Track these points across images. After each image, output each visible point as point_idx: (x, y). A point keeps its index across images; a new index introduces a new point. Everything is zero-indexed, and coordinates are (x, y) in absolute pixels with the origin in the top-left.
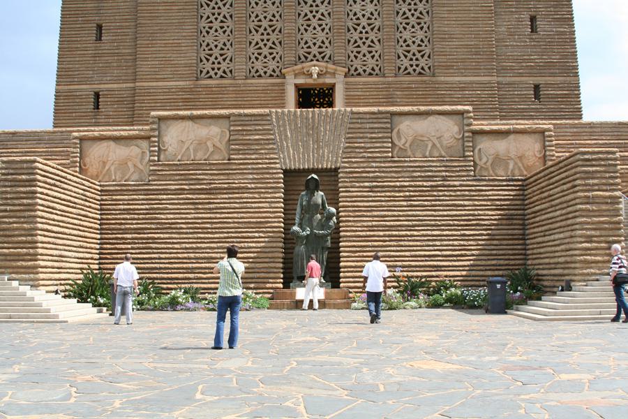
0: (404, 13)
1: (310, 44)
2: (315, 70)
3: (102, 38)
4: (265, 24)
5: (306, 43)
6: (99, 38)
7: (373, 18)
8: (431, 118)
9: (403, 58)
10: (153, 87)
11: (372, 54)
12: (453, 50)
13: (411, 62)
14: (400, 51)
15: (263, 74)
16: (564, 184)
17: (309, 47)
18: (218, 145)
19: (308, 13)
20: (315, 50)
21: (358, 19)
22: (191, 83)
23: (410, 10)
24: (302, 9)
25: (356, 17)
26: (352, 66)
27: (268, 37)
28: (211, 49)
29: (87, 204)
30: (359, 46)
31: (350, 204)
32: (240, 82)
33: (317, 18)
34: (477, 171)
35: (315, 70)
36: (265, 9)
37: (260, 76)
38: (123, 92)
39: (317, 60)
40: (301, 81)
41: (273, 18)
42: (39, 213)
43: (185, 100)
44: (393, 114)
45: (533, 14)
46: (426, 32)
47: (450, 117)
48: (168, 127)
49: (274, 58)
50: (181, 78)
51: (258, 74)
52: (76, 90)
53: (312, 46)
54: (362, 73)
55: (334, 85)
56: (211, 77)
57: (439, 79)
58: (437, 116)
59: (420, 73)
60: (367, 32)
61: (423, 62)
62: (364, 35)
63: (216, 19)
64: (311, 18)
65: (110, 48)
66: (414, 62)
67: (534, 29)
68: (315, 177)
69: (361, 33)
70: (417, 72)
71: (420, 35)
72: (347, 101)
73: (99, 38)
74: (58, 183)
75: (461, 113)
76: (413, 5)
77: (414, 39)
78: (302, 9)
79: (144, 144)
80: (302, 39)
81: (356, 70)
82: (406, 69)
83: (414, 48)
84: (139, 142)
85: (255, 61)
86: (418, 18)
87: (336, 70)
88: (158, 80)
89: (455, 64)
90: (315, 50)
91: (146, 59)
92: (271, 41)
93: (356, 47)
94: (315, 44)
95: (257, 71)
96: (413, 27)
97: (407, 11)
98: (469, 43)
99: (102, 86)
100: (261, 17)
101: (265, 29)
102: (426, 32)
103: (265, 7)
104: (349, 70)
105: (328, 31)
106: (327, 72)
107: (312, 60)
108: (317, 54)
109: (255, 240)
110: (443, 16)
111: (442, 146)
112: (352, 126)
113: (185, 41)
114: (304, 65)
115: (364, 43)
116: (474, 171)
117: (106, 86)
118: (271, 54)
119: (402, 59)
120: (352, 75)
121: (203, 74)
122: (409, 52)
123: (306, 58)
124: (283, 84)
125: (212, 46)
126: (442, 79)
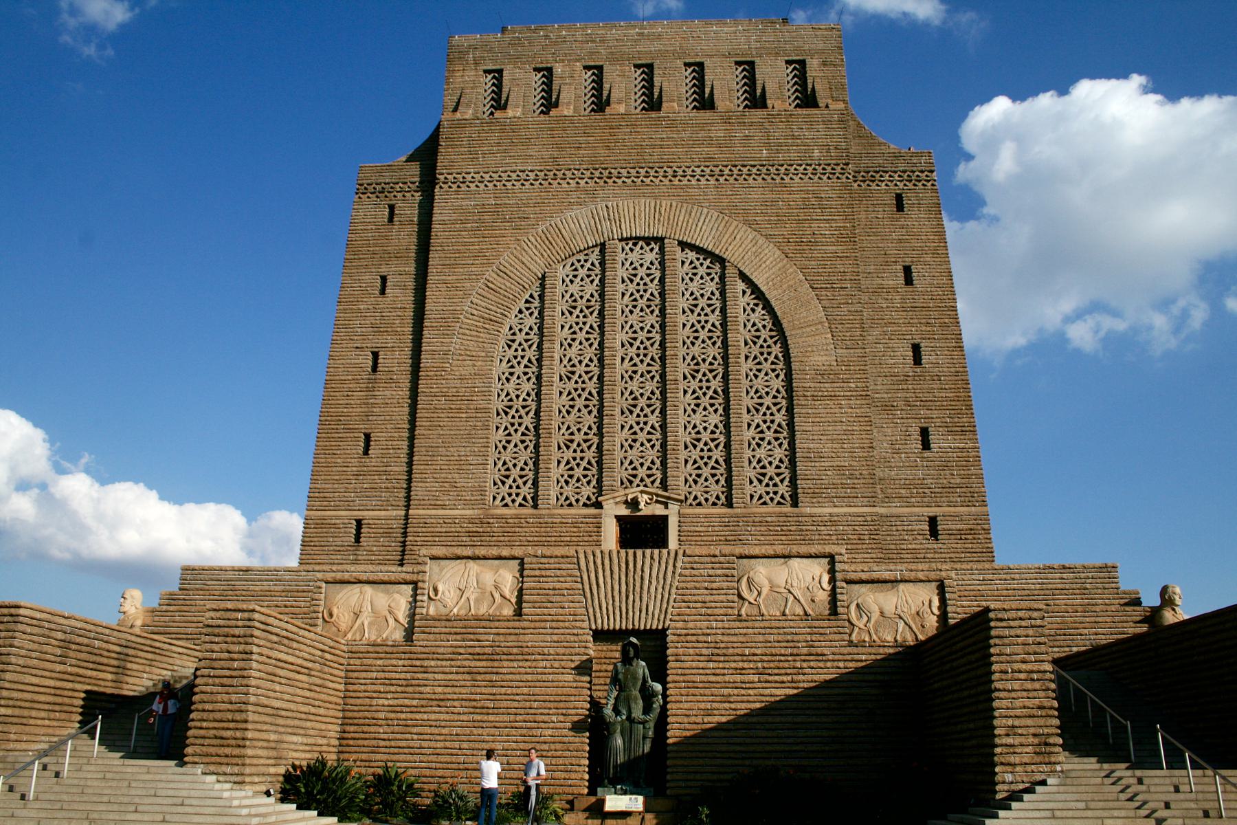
0: (758, 426)
3: (370, 452)
4: (578, 438)
5: (631, 463)
6: (366, 452)
8: (795, 563)
9: (756, 482)
10: (430, 516)
11: (716, 478)
12: (821, 472)
13: (768, 489)
14: (752, 474)
15: (574, 503)
16: (970, 653)
17: (635, 469)
18: (507, 594)
21: (698, 433)
22: (480, 512)
23: (765, 422)
24: (626, 419)
25: (696, 430)
26: (690, 493)
27: (582, 455)
28: (508, 469)
29: (326, 669)
30: (699, 468)
31: (681, 678)
32: (544, 512)
34: (854, 635)
35: (643, 499)
36: (579, 420)
37: (570, 505)
38: (393, 522)
39: (645, 486)
40: (624, 511)
41: (589, 431)
42: (253, 682)
43: (471, 534)
44: (740, 557)
45: (924, 425)
47: (818, 560)
48: (441, 570)
49: (589, 483)
50: (468, 504)
51: (568, 502)
52: (331, 517)
54: (703, 502)
55: (667, 516)
56: (506, 505)
57: (803, 510)
58: (799, 559)
59: (779, 503)
62: (706, 454)
63: (516, 431)
65: (376, 464)
66: (770, 489)
67: (926, 445)
68: (634, 640)
70: (776, 502)
73: (366, 452)
74: (286, 641)
75: (831, 558)
78: (626, 419)
79: (408, 589)
80: (625, 458)
81: (695, 498)
82: (761, 497)
83: (771, 471)
84: (404, 587)
85: (564, 484)
87: (669, 498)
88: (436, 507)
89: (825, 491)
91: (423, 480)
92: (586, 461)
94: (642, 465)
95: (567, 498)
96: (769, 443)
98: (843, 464)
99: (365, 513)
100: (574, 429)
101: (579, 445)
103: (579, 417)
104: (686, 498)
106: (657, 502)
107: (638, 486)
109: (551, 725)
110: (807, 429)
111: (806, 600)
112: (684, 571)
113: (475, 458)
114: (627, 491)
115: (706, 464)
116: (850, 635)
117: (371, 513)
118: (585, 476)
119: (754, 484)
120: (691, 505)
121: (498, 502)
122: (764, 475)
123: (631, 482)
124: (599, 516)
125: (510, 465)
126: (808, 510)
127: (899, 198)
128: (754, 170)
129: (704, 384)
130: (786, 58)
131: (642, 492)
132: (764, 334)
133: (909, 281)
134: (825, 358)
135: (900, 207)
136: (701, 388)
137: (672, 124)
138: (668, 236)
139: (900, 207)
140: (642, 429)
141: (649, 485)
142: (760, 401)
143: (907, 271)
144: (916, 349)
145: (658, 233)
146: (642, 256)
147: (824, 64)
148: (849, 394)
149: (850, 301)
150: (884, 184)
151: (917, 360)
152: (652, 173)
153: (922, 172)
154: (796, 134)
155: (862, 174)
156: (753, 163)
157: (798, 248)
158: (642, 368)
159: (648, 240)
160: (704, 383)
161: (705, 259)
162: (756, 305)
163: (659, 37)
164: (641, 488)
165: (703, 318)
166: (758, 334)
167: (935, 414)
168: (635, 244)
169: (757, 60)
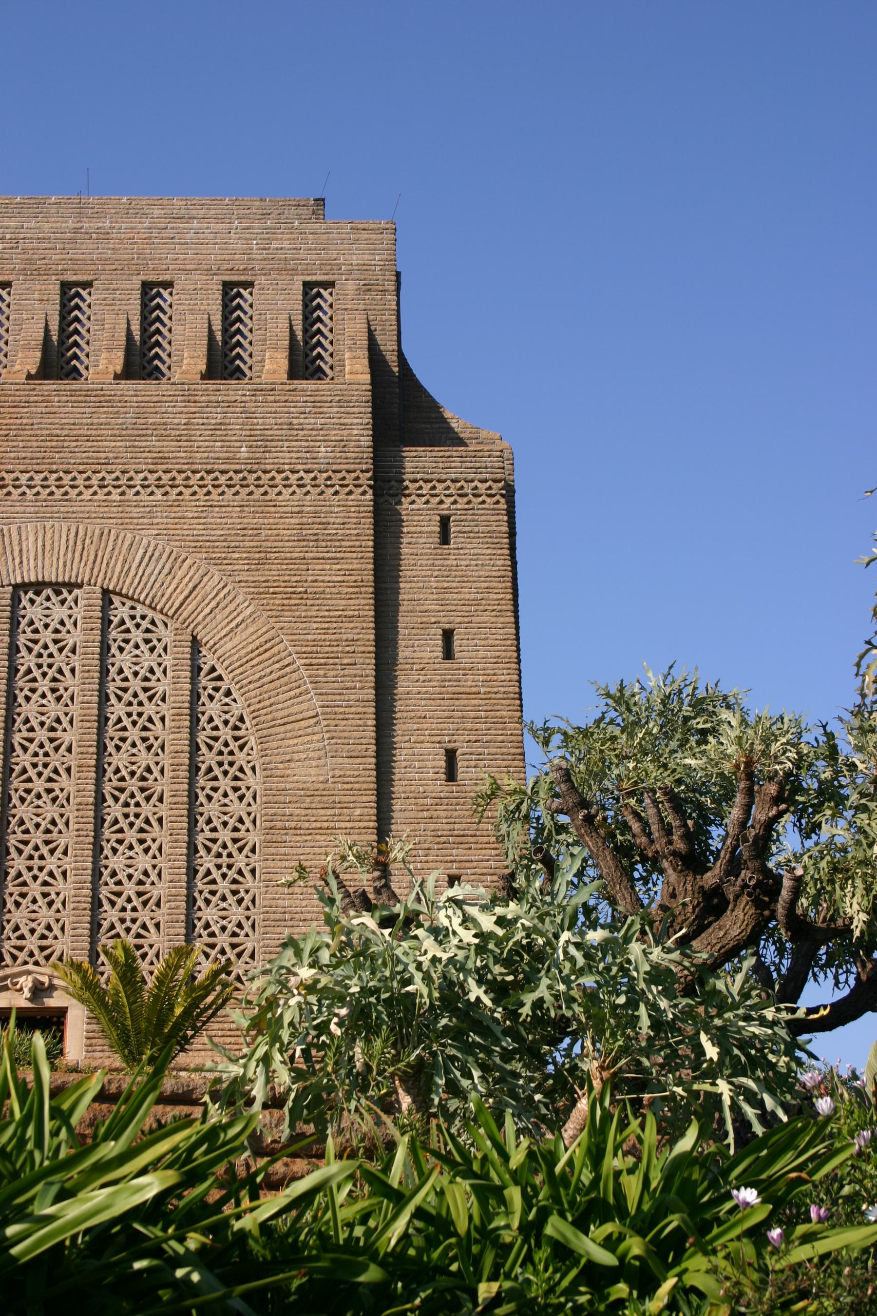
1: (24, 930)
2: (26, 982)
7: (149, 881)
19: (24, 872)
20: (32, 943)
23: (219, 867)
33: (39, 881)
39: (37, 963)
46: (248, 909)
53: (27, 935)
60: (134, 909)
61: (239, 967)
62: (128, 915)
64: (29, 881)
69: (124, 909)
71: (237, 914)
72: (89, 1042)
76: (225, 857)
77: (224, 922)
86: (235, 881)
90: (32, 943)
93: (112, 937)
94: (33, 931)
97: (213, 870)
102: (248, 909)
105: (60, 906)
107: (26, 963)
108: (36, 952)
123: (15, 958)
127: (445, 522)
128: (223, 479)
129: (132, 810)
130: (309, 278)
131: (29, 973)
132: (225, 733)
133: (448, 654)
134: (313, 771)
135: (445, 538)
136: (126, 816)
137: (104, 401)
138: (86, 580)
139: (445, 538)
140: (35, 878)
141: (42, 961)
142: (214, 835)
143: (448, 635)
144: (451, 755)
145: (77, 577)
146: (47, 612)
147: (368, 288)
148: (349, 825)
149: (358, 685)
150: (424, 499)
151: (451, 775)
152: (67, 481)
153: (485, 481)
154: (295, 421)
155: (393, 483)
156: (223, 467)
157: (286, 602)
158: (39, 785)
159: (58, 587)
160: (132, 807)
161: (143, 617)
162: (216, 689)
163: (105, 235)
164: (30, 967)
165: (135, 709)
166: (215, 733)
167: (474, 855)
168: (38, 593)
169: (260, 281)
